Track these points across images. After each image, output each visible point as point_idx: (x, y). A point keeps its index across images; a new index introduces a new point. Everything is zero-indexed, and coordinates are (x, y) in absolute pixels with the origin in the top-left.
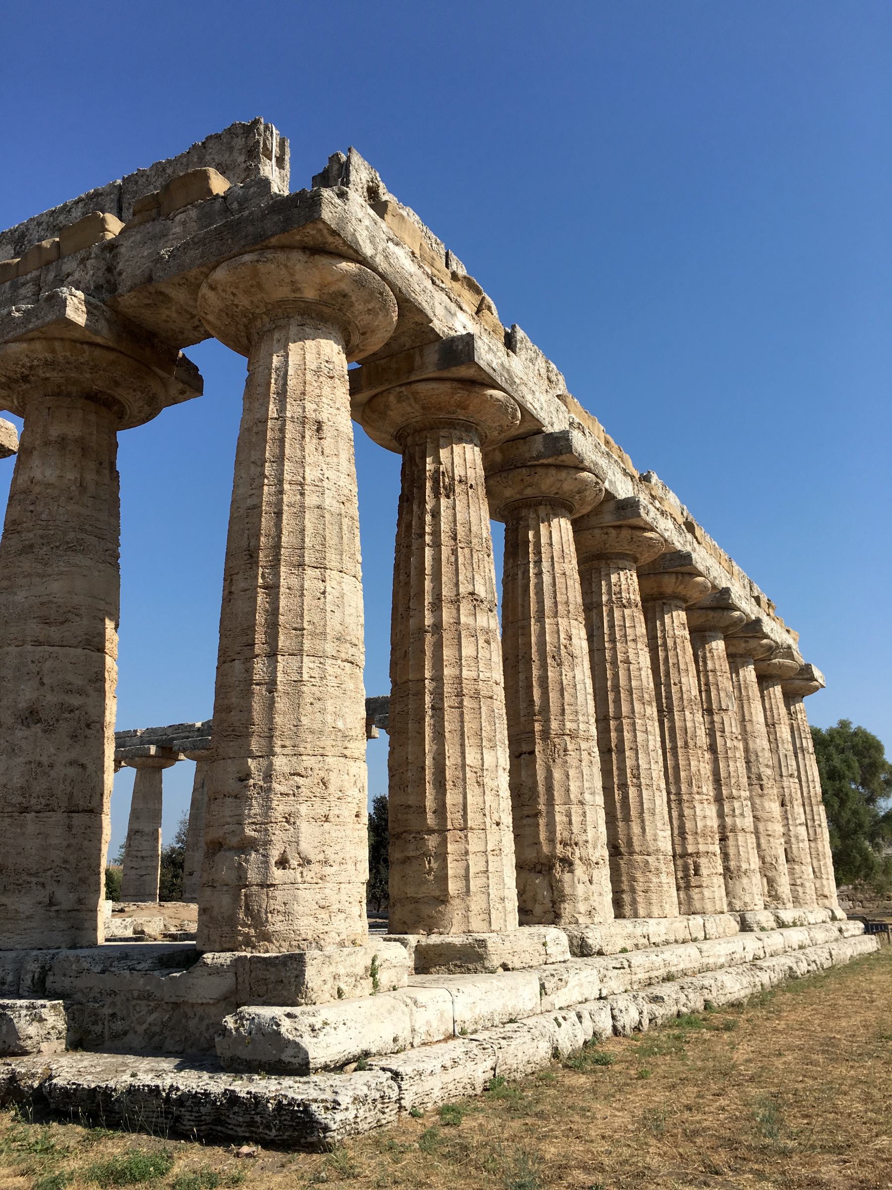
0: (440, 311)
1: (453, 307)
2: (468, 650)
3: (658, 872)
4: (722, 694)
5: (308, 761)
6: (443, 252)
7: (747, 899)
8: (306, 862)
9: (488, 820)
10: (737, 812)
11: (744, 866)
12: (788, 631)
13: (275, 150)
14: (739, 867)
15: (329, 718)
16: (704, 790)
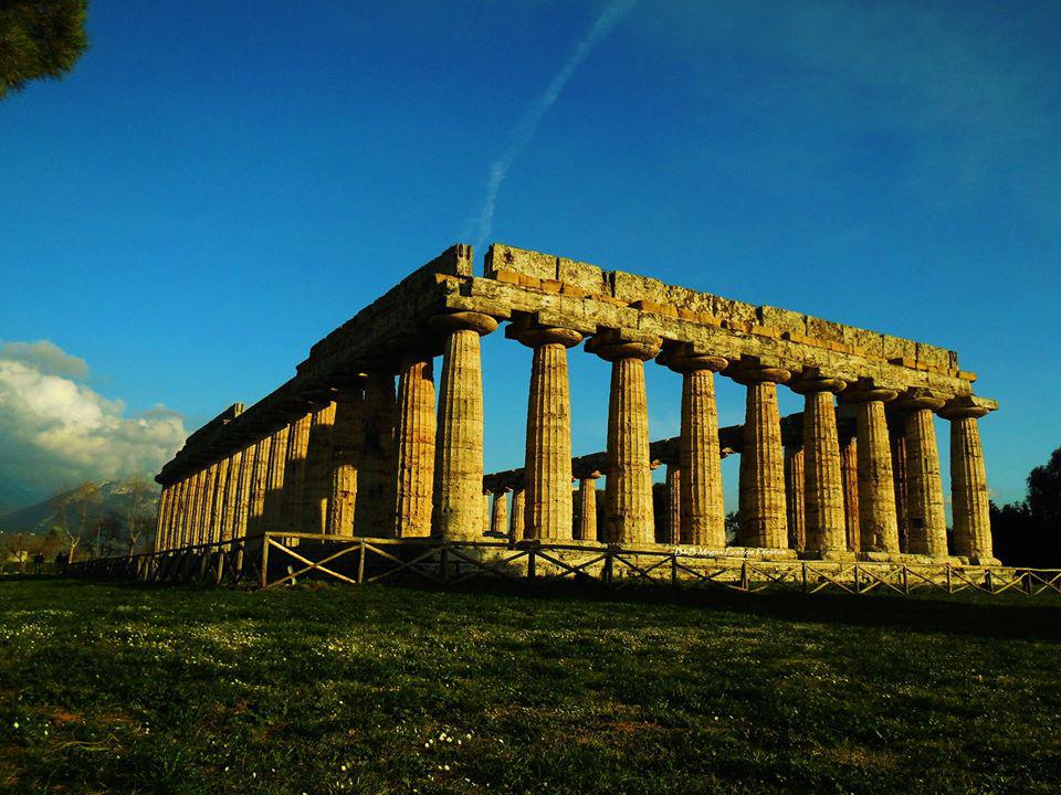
0: (530, 302)
1: (540, 296)
2: (545, 435)
3: (705, 524)
4: (822, 429)
5: (452, 481)
6: (554, 261)
7: (828, 544)
8: (451, 511)
9: (551, 500)
10: (825, 496)
11: (827, 526)
12: (958, 376)
13: (465, 253)
14: (824, 527)
15: (460, 468)
16: (772, 485)
